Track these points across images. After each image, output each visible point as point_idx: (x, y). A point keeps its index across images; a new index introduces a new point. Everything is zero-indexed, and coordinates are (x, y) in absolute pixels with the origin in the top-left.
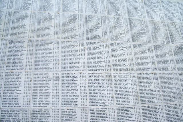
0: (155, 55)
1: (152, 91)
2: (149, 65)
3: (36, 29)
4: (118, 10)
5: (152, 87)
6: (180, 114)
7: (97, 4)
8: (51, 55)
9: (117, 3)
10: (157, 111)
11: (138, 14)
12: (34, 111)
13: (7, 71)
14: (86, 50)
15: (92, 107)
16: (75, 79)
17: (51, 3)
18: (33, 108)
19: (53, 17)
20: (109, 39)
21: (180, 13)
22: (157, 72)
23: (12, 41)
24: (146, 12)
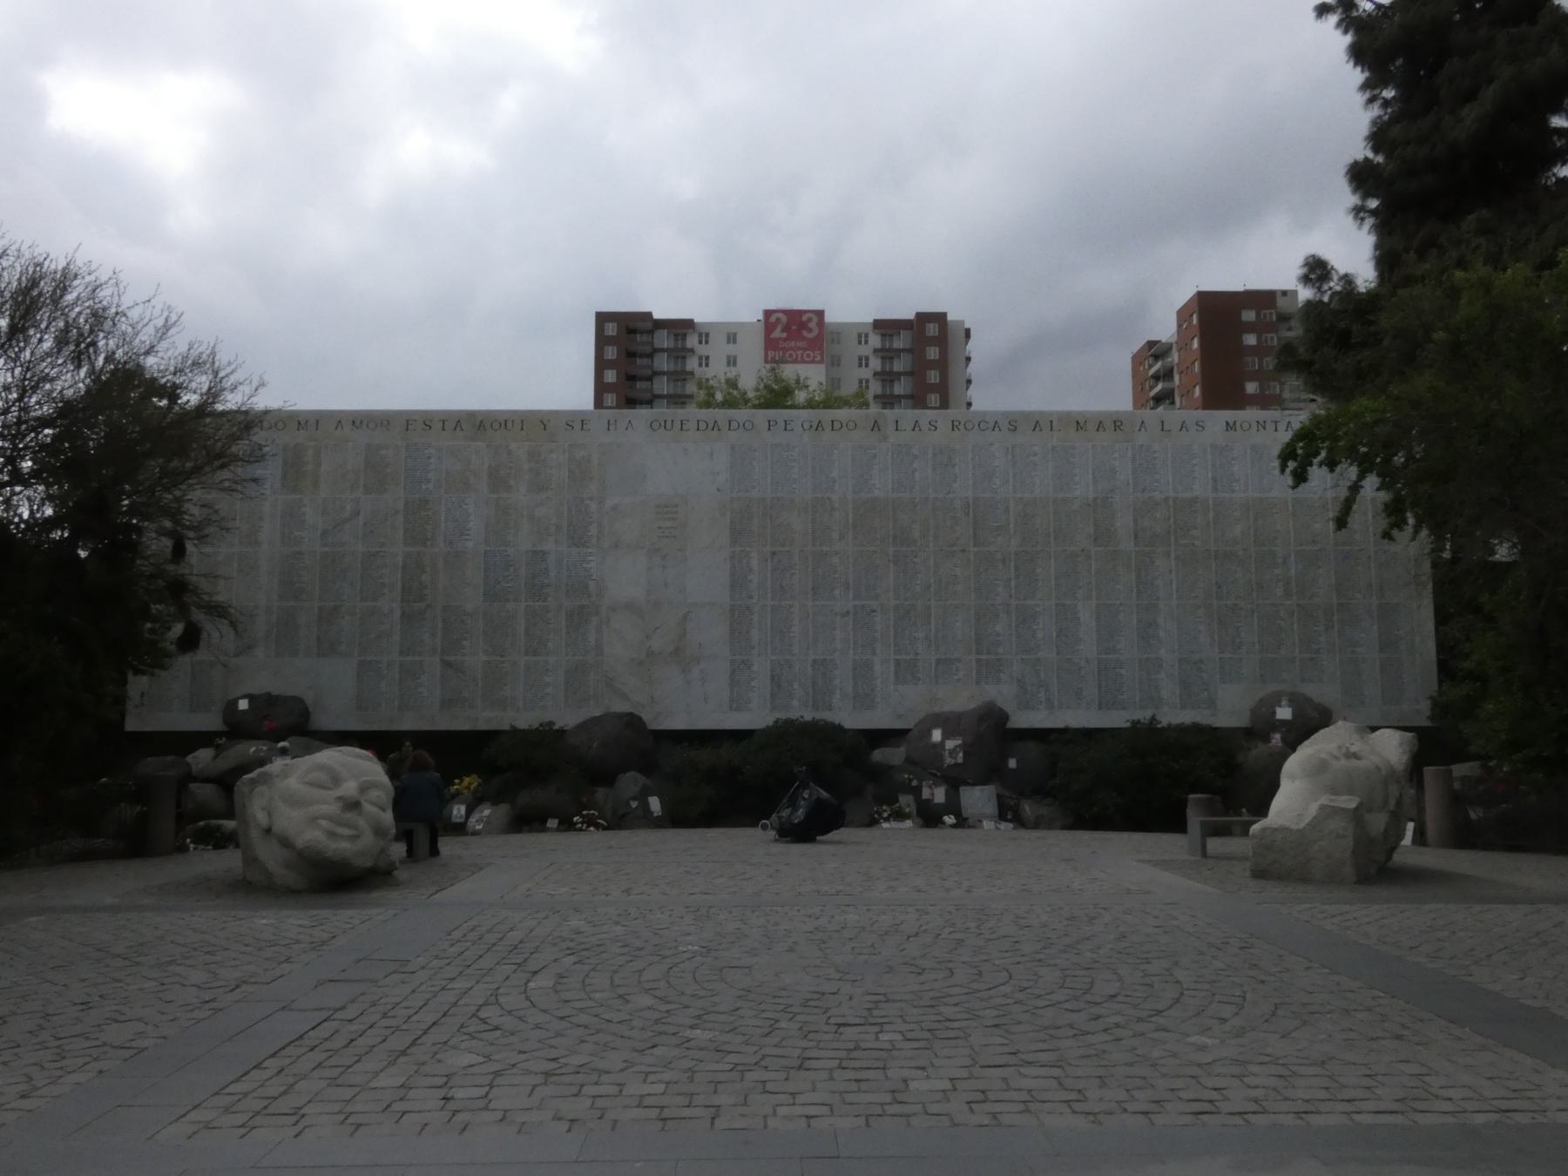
0: (1012, 570)
1: (998, 635)
2: (1000, 589)
3: (810, 531)
4: (955, 481)
5: (998, 628)
6: (1042, 675)
7: (915, 471)
8: (836, 576)
9: (953, 466)
10: (1001, 668)
11: (995, 487)
12: (815, 661)
13: (773, 603)
14: (891, 565)
15: (898, 657)
16: (874, 614)
17: (832, 475)
18: (813, 658)
19: (836, 505)
20: (931, 545)
21: (1090, 472)
22: (1013, 602)
23: (774, 553)
24: (1011, 480)
